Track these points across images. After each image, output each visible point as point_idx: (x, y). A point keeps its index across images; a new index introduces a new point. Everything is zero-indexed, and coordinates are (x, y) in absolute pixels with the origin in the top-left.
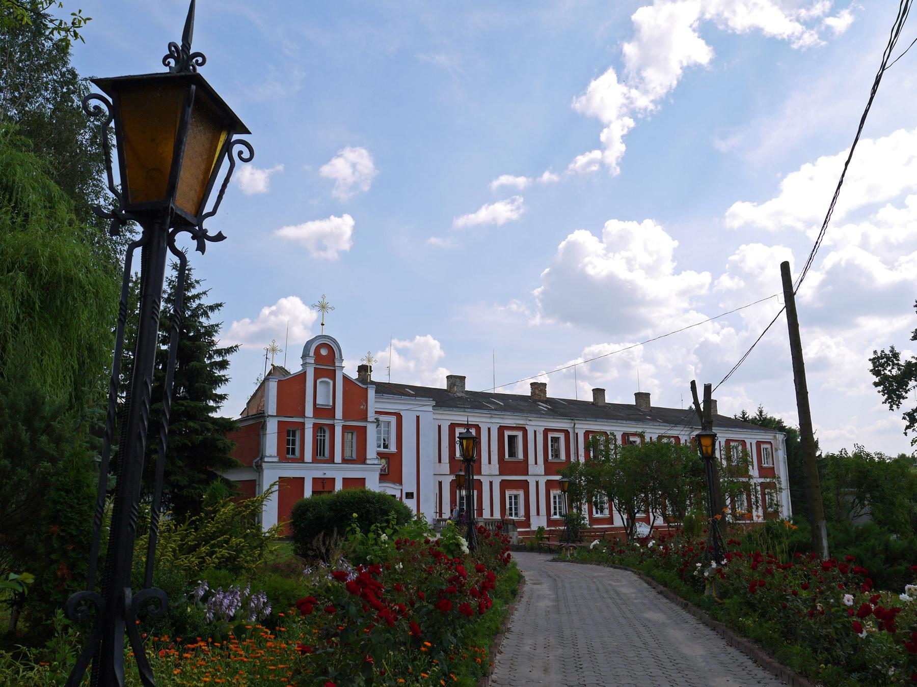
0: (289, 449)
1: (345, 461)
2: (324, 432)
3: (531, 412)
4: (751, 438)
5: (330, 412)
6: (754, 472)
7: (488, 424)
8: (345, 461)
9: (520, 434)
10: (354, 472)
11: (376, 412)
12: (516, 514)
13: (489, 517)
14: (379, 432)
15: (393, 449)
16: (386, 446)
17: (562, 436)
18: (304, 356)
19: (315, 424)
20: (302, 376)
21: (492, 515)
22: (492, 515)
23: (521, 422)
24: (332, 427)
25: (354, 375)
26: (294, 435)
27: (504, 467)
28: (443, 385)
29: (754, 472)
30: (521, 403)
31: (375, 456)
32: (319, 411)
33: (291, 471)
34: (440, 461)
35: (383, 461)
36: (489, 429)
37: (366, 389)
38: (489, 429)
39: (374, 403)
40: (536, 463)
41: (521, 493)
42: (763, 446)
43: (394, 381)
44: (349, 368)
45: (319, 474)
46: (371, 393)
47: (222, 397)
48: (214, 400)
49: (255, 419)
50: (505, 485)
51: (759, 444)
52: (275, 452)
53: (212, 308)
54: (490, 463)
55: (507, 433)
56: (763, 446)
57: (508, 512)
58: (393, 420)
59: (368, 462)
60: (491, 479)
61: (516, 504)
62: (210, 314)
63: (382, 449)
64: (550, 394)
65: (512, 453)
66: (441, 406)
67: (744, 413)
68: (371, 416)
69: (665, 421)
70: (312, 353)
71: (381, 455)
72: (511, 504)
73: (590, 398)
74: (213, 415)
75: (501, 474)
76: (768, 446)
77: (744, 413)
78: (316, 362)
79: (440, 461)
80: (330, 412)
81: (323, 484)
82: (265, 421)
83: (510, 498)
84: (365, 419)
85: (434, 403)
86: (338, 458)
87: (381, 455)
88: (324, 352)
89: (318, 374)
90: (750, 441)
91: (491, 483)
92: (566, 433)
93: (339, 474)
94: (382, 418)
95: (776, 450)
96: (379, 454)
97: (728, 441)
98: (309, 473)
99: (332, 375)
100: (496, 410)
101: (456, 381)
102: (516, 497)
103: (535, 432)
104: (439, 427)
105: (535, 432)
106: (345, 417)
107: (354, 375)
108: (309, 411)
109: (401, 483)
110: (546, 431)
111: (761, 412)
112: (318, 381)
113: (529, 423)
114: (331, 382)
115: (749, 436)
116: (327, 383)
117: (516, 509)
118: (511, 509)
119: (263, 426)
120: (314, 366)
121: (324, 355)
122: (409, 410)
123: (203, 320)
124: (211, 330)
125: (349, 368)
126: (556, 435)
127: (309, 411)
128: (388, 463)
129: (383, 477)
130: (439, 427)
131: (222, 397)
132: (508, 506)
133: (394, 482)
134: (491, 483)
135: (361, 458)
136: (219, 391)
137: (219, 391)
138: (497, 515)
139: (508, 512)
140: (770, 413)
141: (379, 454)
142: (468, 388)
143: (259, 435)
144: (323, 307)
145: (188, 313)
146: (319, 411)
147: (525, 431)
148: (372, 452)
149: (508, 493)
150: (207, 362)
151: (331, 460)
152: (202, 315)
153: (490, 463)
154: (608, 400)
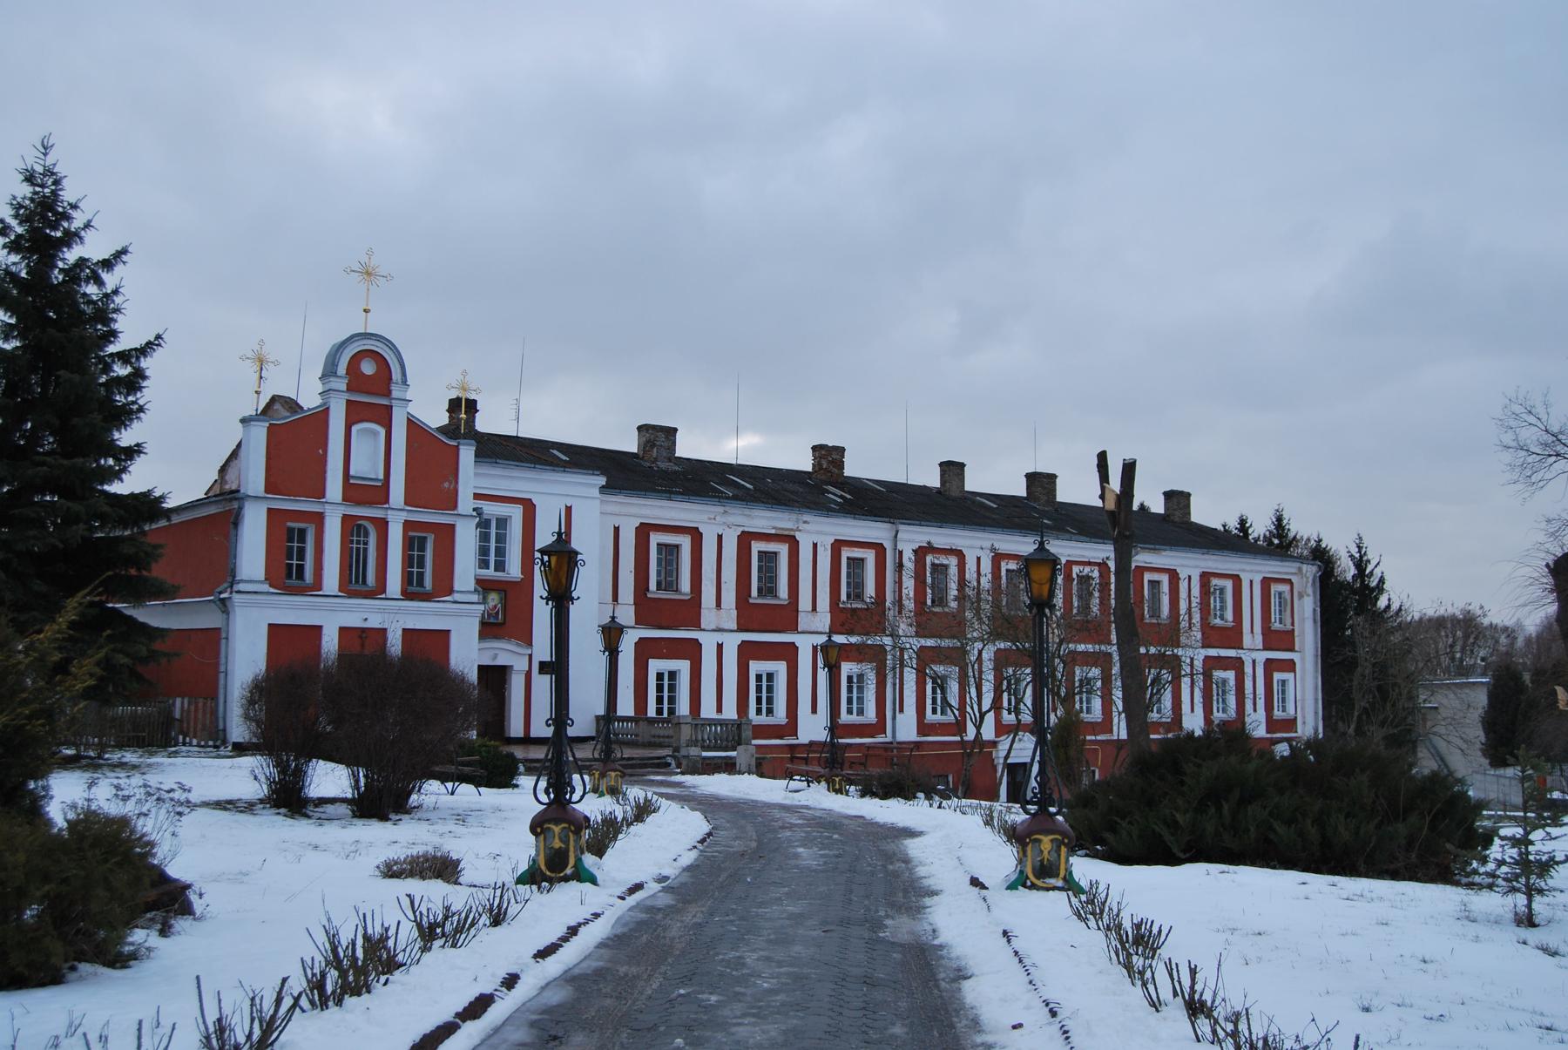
0: (289, 571)
1: (407, 595)
2: (366, 534)
4: (1253, 571)
5: (377, 493)
6: (1252, 637)
7: (720, 524)
9: (783, 550)
10: (424, 616)
11: (477, 496)
13: (714, 715)
16: (500, 566)
17: (870, 556)
18: (329, 372)
19: (345, 518)
20: (322, 415)
21: (719, 710)
22: (719, 710)
24: (382, 525)
25: (436, 417)
26: (302, 539)
27: (749, 617)
29: (1252, 637)
30: (791, 487)
31: (471, 585)
32: (356, 491)
33: (294, 611)
35: (494, 599)
36: (720, 537)
37: (457, 448)
38: (720, 537)
39: (472, 476)
40: (814, 609)
42: (1275, 588)
45: (354, 621)
46: (467, 454)
47: (133, 452)
48: (117, 459)
49: (223, 505)
50: (747, 652)
51: (1266, 583)
52: (260, 573)
53: (107, 264)
54: (719, 605)
56: (1275, 588)
60: (719, 637)
62: (105, 276)
63: (490, 573)
64: (851, 469)
68: (466, 503)
70: (342, 369)
71: (484, 586)
73: (934, 481)
74: (116, 488)
75: (741, 629)
76: (1285, 588)
78: (350, 389)
80: (377, 493)
81: (360, 640)
82: (241, 508)
83: (759, 677)
85: (602, 481)
89: (356, 413)
91: (720, 647)
92: (879, 549)
93: (395, 618)
94: (491, 509)
95: (1301, 596)
98: (332, 617)
99: (383, 417)
100: (735, 498)
101: (658, 437)
102: (770, 676)
103: (815, 545)
104: (617, 530)
105: (815, 545)
107: (436, 417)
108: (334, 489)
109: (530, 644)
110: (837, 546)
112: (355, 429)
114: (382, 431)
115: (1248, 567)
116: (375, 434)
117: (770, 700)
119: (233, 520)
120: (347, 396)
123: (91, 289)
124: (103, 313)
126: (857, 553)
127: (334, 489)
129: (490, 629)
130: (617, 530)
131: (133, 452)
134: (720, 647)
136: (125, 438)
137: (125, 438)
138: (730, 712)
143: (227, 536)
144: (368, 273)
145: (57, 277)
150: (103, 379)
151: (379, 591)
152: (87, 281)
153: (719, 605)
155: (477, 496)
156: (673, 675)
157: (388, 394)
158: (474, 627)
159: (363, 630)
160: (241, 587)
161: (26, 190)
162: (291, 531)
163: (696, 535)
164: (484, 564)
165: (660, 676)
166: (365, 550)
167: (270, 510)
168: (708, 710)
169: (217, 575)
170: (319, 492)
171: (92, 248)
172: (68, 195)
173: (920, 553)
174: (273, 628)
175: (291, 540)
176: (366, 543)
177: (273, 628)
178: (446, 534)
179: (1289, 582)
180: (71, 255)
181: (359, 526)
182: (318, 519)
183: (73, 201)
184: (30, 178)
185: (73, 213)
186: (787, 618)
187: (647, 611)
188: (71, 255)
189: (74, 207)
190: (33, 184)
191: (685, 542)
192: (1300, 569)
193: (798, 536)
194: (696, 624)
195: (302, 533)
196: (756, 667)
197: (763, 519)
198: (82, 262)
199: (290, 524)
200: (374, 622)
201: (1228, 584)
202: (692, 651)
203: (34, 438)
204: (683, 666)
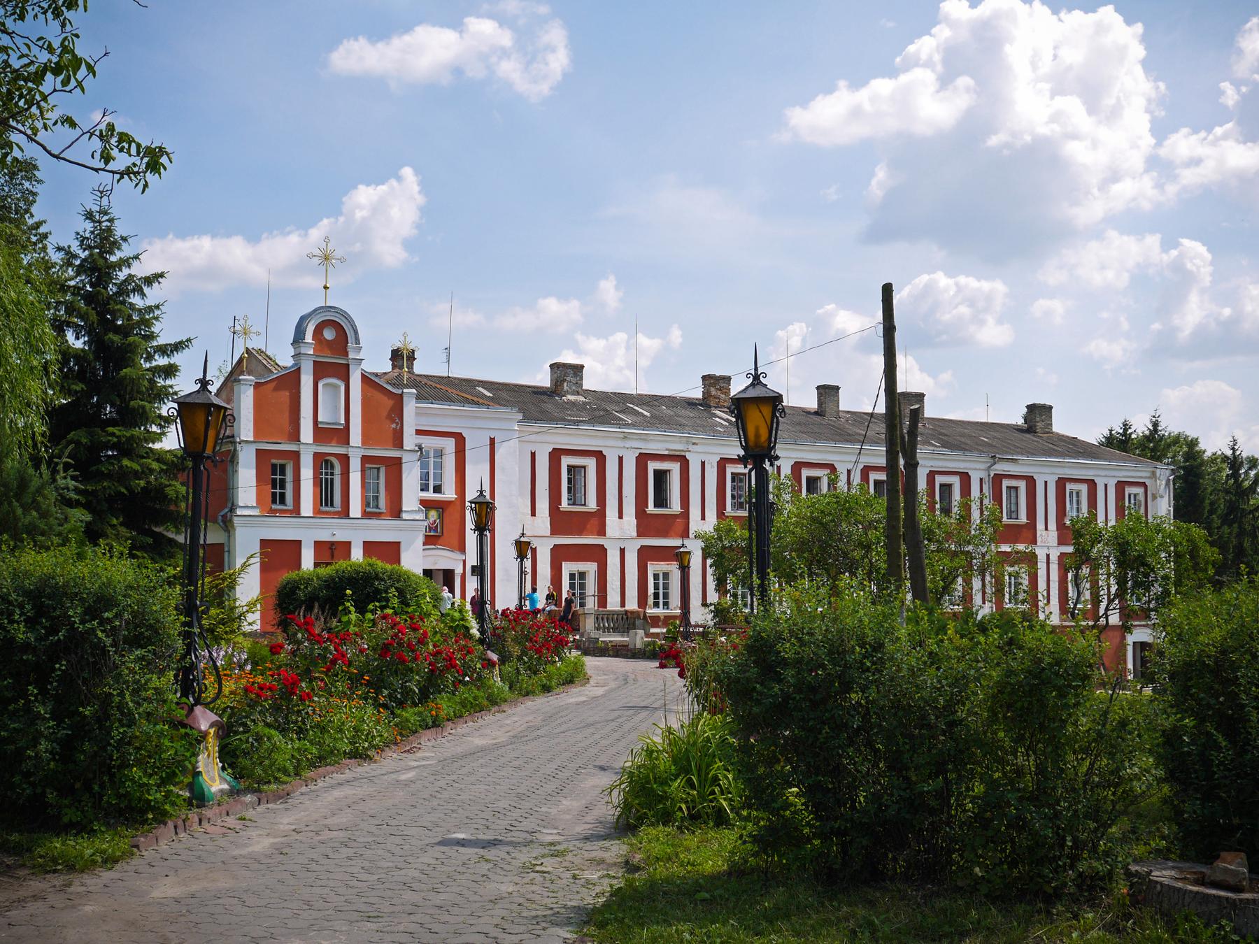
1: (366, 515)
2: (332, 467)
3: (696, 428)
4: (1107, 474)
7: (621, 446)
8: (366, 515)
9: (675, 468)
11: (419, 432)
12: (666, 604)
14: (424, 466)
15: (449, 494)
16: (437, 489)
18: (298, 338)
19: (316, 455)
21: (623, 604)
22: (623, 604)
23: (676, 446)
24: (345, 460)
26: (283, 472)
27: (646, 525)
28: (543, 379)
31: (416, 506)
34: (533, 514)
35: (433, 514)
36: (621, 459)
37: (401, 396)
38: (621, 459)
41: (673, 569)
42: (1128, 490)
43: (458, 372)
44: (373, 358)
45: (325, 536)
50: (646, 555)
51: (1121, 486)
53: (149, 281)
55: (652, 466)
56: (1128, 490)
57: (651, 600)
58: (449, 445)
59: (405, 516)
61: (666, 587)
63: (430, 495)
65: (661, 501)
66: (536, 420)
67: (1126, 426)
68: (410, 440)
69: (945, 445)
70: (309, 338)
71: (427, 505)
72: (656, 587)
76: (1140, 490)
77: (1126, 426)
79: (533, 514)
80: (342, 435)
81: (330, 550)
82: (235, 450)
83: (656, 577)
84: (398, 442)
85: (520, 416)
86: (356, 509)
87: (427, 505)
88: (329, 334)
89: (321, 371)
90: (1105, 480)
93: (357, 533)
94: (428, 442)
95: (1154, 497)
96: (423, 502)
97: (1061, 483)
98: (308, 530)
100: (633, 425)
101: (567, 374)
102: (666, 575)
103: (703, 464)
104: (533, 455)
105: (703, 464)
106: (367, 439)
108: (307, 434)
111: (1156, 425)
113: (691, 447)
117: (666, 596)
118: (656, 595)
121: (332, 339)
122: (476, 426)
123: (136, 300)
124: (148, 316)
125: (373, 358)
127: (307, 434)
128: (441, 517)
129: (431, 540)
130: (533, 455)
132: (651, 590)
133: (452, 549)
135: (396, 511)
138: (632, 605)
139: (651, 600)
140: (1171, 426)
141: (423, 502)
142: (587, 384)
143: (225, 471)
145: (112, 289)
146: (322, 433)
147: (684, 462)
148: (411, 496)
149: (652, 568)
151: (345, 513)
152: (134, 291)
154: (845, 405)
155: (419, 432)
156: (582, 575)
157: (346, 354)
158: (421, 539)
159: (332, 543)
160: (239, 512)
161: (89, 226)
162: (274, 466)
163: (600, 457)
164: (424, 488)
165: (572, 576)
166: (332, 480)
167: (259, 452)
168: (613, 603)
169: (215, 502)
170: (295, 436)
171: (139, 270)
172: (120, 230)
173: (798, 467)
174: (264, 543)
175: (274, 473)
176: (332, 474)
177: (264, 543)
178: (394, 466)
179: (1144, 485)
180: (122, 275)
181: (327, 461)
182: (296, 456)
183: (124, 235)
184: (89, 216)
185: (124, 246)
186: (679, 525)
187: (560, 522)
188: (122, 275)
189: (124, 239)
190: (94, 221)
191: (591, 463)
192: (1154, 473)
193: (688, 456)
194: (602, 532)
195: (283, 468)
196: (652, 568)
197: (659, 442)
198: (130, 277)
199: (274, 461)
200: (340, 537)
201: (1084, 489)
202: (598, 554)
203: (100, 406)
204: (591, 568)
